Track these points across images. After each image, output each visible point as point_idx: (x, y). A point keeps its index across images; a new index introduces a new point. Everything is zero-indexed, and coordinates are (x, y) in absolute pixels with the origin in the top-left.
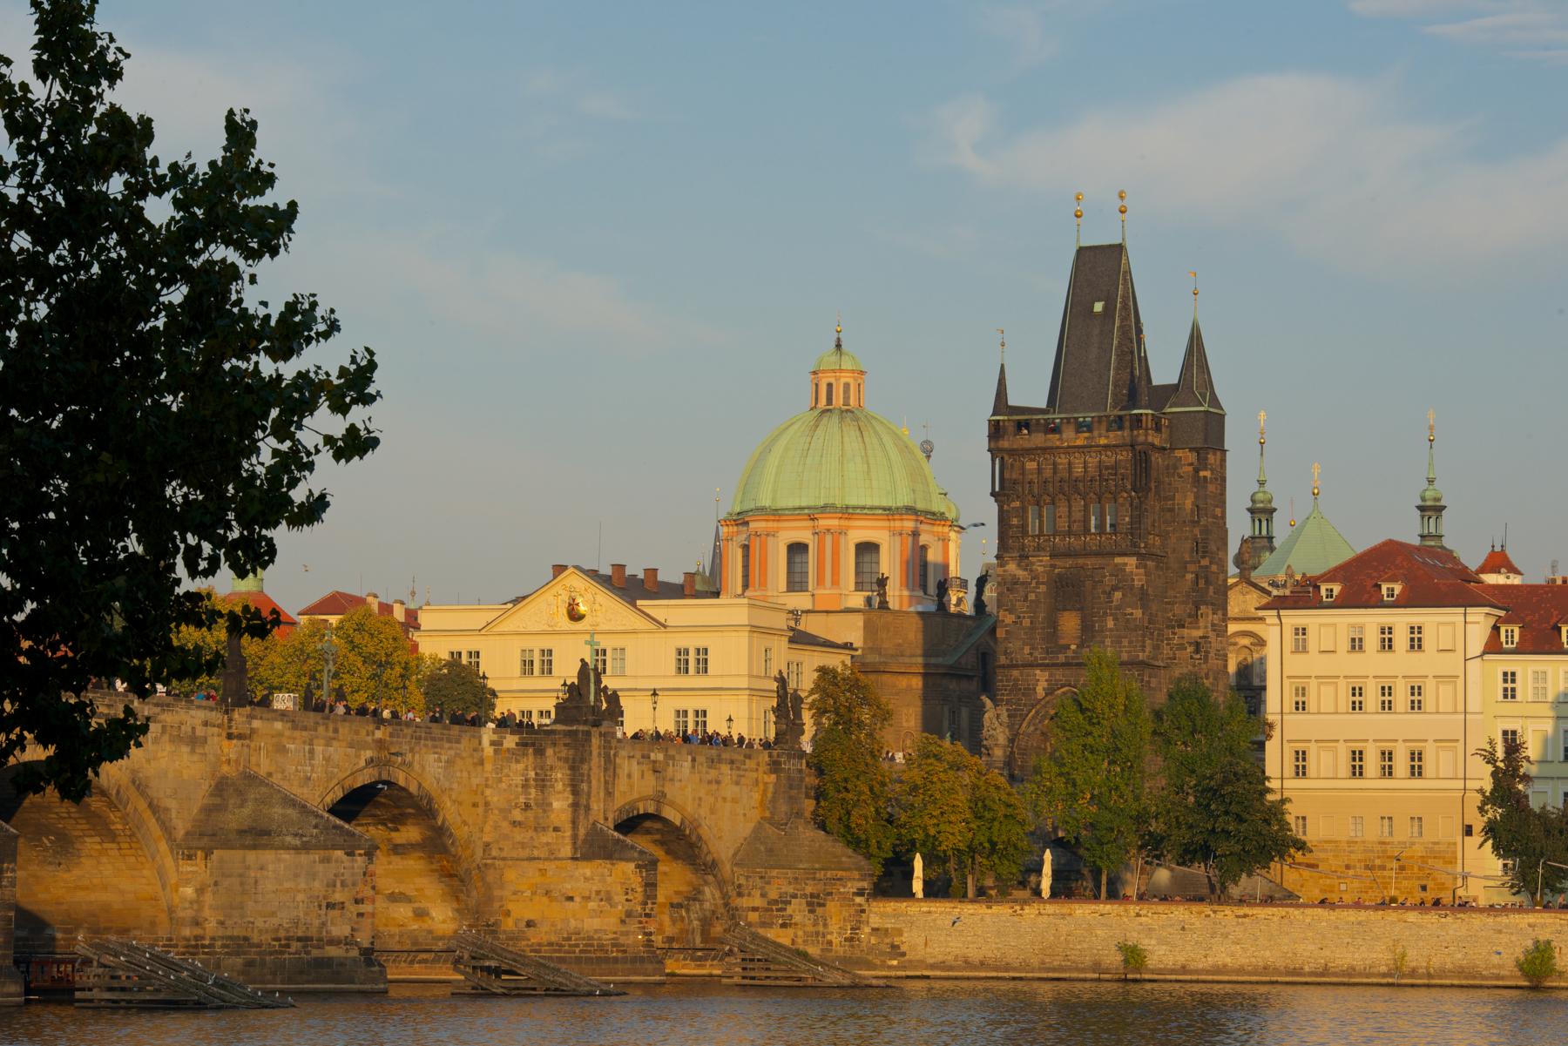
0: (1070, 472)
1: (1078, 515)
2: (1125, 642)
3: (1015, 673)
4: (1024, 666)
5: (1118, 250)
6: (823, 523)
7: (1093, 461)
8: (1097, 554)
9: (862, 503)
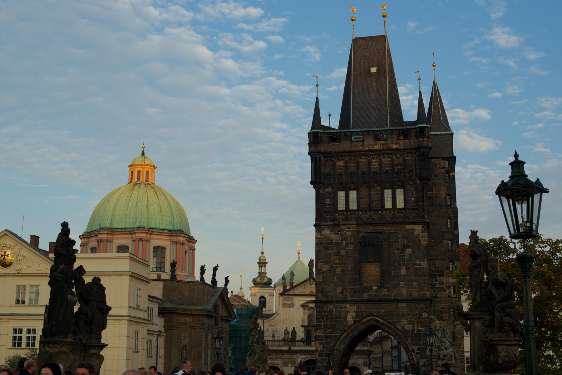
0: (369, 168)
2: (415, 284)
3: (331, 306)
4: (337, 302)
5: (384, 38)
6: (138, 235)
7: (386, 161)
8: (392, 223)
9: (157, 227)
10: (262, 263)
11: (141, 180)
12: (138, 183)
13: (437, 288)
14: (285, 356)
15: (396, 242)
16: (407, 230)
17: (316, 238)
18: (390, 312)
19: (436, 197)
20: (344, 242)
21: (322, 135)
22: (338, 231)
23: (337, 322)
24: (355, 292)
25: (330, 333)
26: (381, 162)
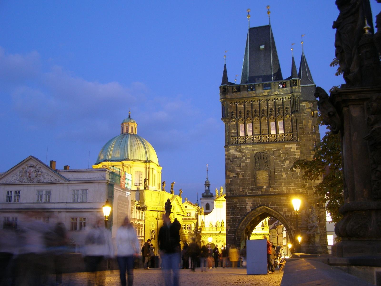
1: (264, 127)
2: (292, 184)
3: (236, 200)
5: (268, 28)
7: (271, 103)
10: (207, 185)
13: (307, 187)
15: (279, 156)
16: (286, 148)
17: (226, 155)
18: (275, 203)
19: (305, 127)
20: (244, 157)
21: (229, 88)
22: (240, 150)
23: (240, 210)
24: (252, 190)
25: (236, 218)
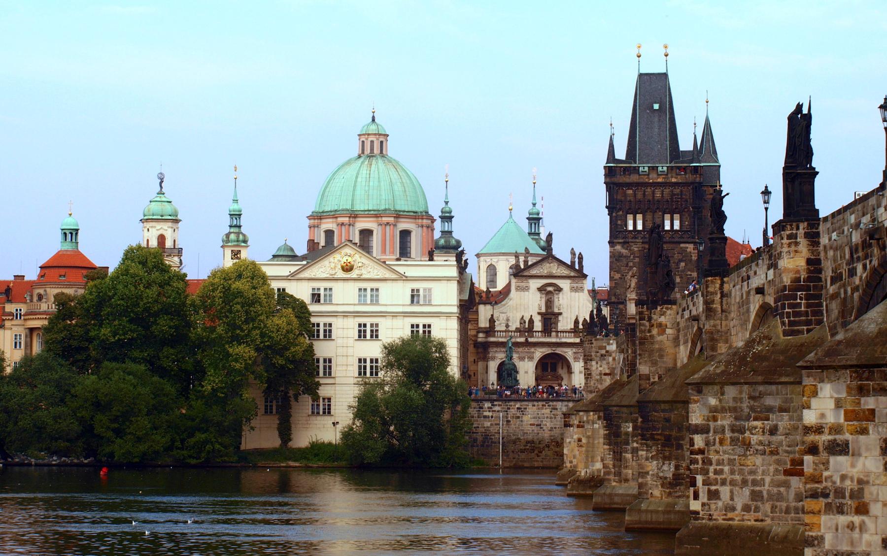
5: (665, 75)
9: (403, 209)
11: (375, 152)
12: (371, 156)
14: (520, 350)
26: (663, 191)
